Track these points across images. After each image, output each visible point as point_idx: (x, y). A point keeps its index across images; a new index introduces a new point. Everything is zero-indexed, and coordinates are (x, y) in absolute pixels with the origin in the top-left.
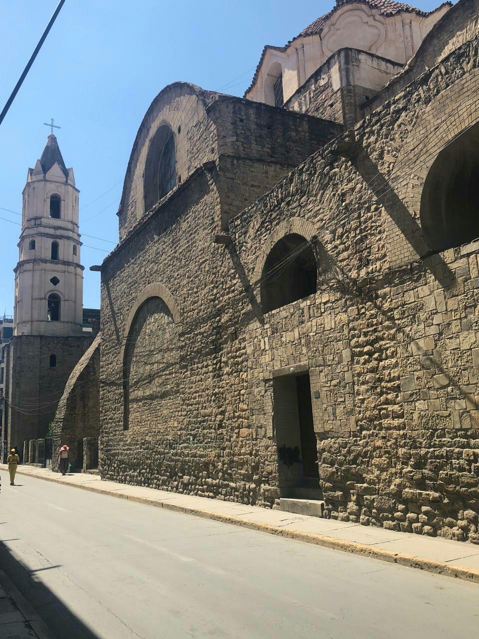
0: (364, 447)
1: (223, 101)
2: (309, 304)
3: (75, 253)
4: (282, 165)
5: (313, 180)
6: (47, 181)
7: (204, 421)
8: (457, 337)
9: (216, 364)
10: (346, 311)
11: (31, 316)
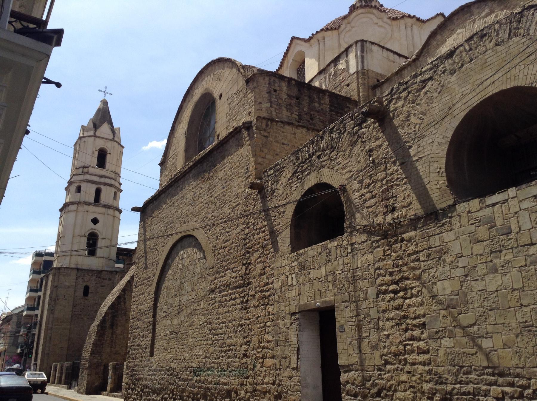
0: (389, 381)
2: (336, 245)
3: (116, 197)
4: (308, 129)
5: (342, 138)
6: (97, 137)
7: (229, 350)
8: (483, 279)
9: (244, 297)
10: (372, 252)
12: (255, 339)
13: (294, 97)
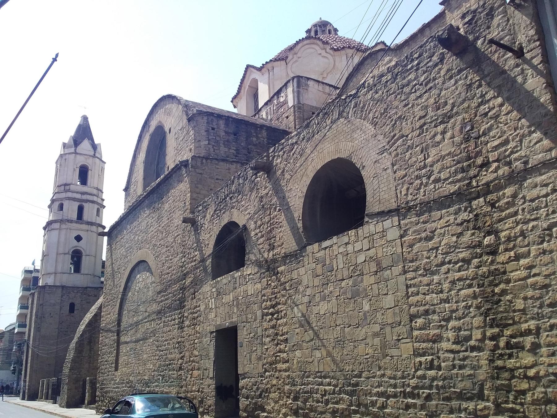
0: (266, 385)
1: (200, 114)
6: (78, 154)
7: (170, 364)
8: (318, 305)
9: (180, 318)
10: (260, 282)
11: (56, 269)
12: (187, 354)
13: (231, 133)
